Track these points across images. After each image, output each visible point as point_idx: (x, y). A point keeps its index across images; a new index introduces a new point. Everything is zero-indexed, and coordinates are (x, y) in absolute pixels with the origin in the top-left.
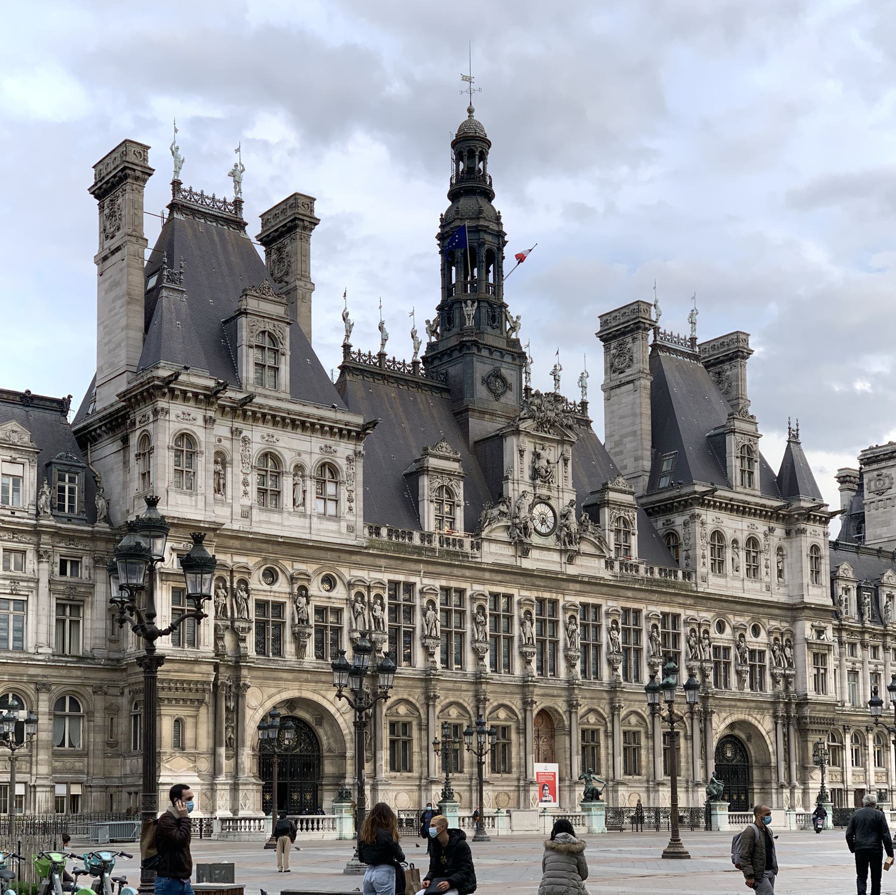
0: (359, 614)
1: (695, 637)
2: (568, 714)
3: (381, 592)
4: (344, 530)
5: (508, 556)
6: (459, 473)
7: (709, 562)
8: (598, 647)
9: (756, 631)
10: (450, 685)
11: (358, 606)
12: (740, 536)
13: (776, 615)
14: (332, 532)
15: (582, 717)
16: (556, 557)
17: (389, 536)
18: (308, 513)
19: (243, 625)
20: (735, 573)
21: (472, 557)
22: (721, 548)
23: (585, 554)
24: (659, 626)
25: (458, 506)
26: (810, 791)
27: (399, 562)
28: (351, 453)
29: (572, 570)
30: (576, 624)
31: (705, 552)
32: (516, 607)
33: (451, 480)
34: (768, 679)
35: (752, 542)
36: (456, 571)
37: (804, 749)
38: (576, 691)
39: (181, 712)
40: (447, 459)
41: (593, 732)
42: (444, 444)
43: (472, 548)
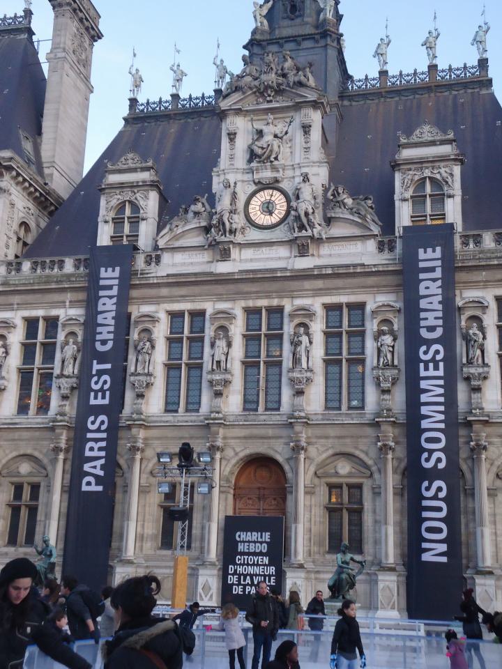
2: (292, 463)
5: (203, 263)
6: (143, 182)
8: (358, 360)
15: (322, 465)
16: (283, 252)
17: (34, 269)
21: (141, 274)
25: (143, 219)
30: (308, 334)
32: (207, 324)
33: (135, 193)
38: (298, 428)
41: (350, 486)
42: (130, 156)
43: (148, 263)
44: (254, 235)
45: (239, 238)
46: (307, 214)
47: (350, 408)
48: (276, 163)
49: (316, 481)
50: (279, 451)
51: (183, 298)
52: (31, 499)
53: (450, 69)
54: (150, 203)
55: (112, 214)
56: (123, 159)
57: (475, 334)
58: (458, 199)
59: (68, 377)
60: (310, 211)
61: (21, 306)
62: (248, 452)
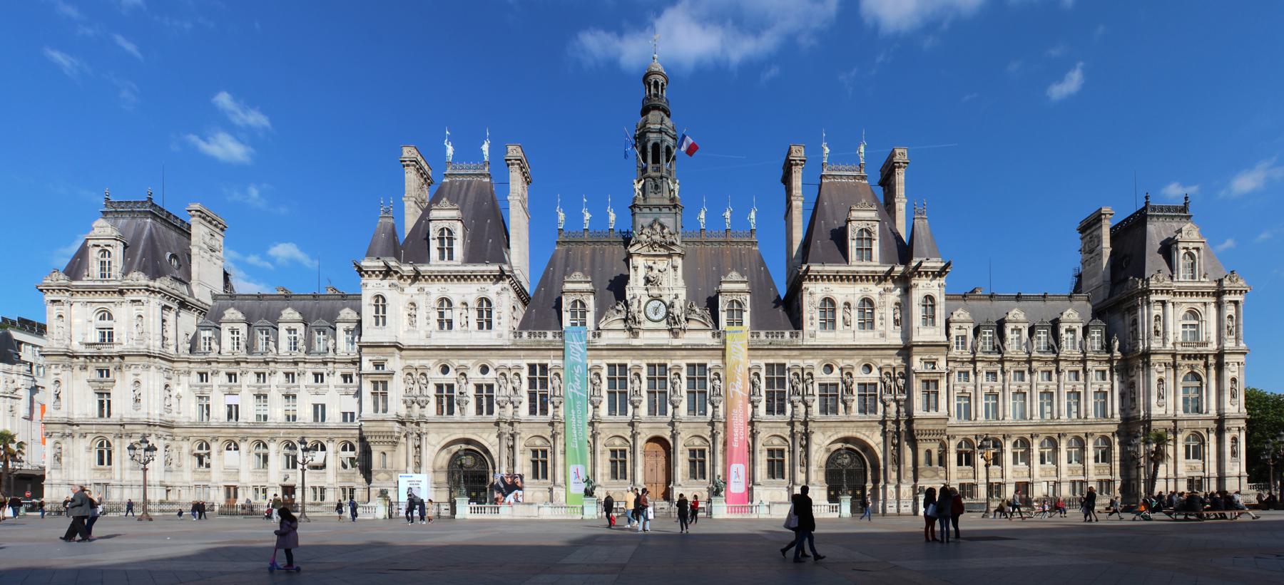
0: (500, 386)
1: (798, 378)
3: (518, 371)
7: (817, 322)
9: (868, 368)
11: (501, 381)
12: (852, 298)
13: (889, 355)
14: (486, 339)
16: (666, 335)
17: (530, 336)
18: (469, 329)
19: (422, 399)
20: (846, 327)
22: (834, 311)
24: (763, 374)
27: (535, 352)
28: (500, 289)
29: (676, 342)
30: (679, 378)
31: (814, 315)
34: (880, 405)
35: (867, 301)
38: (676, 424)
39: (384, 449)
40: (581, 282)
41: (699, 450)
42: (577, 273)
43: (594, 337)
45: (642, 326)
46: (678, 316)
47: (699, 414)
48: (660, 286)
49: (684, 448)
50: (667, 434)
51: (615, 356)
52: (542, 457)
54: (590, 302)
55: (570, 307)
56: (573, 275)
58: (748, 312)
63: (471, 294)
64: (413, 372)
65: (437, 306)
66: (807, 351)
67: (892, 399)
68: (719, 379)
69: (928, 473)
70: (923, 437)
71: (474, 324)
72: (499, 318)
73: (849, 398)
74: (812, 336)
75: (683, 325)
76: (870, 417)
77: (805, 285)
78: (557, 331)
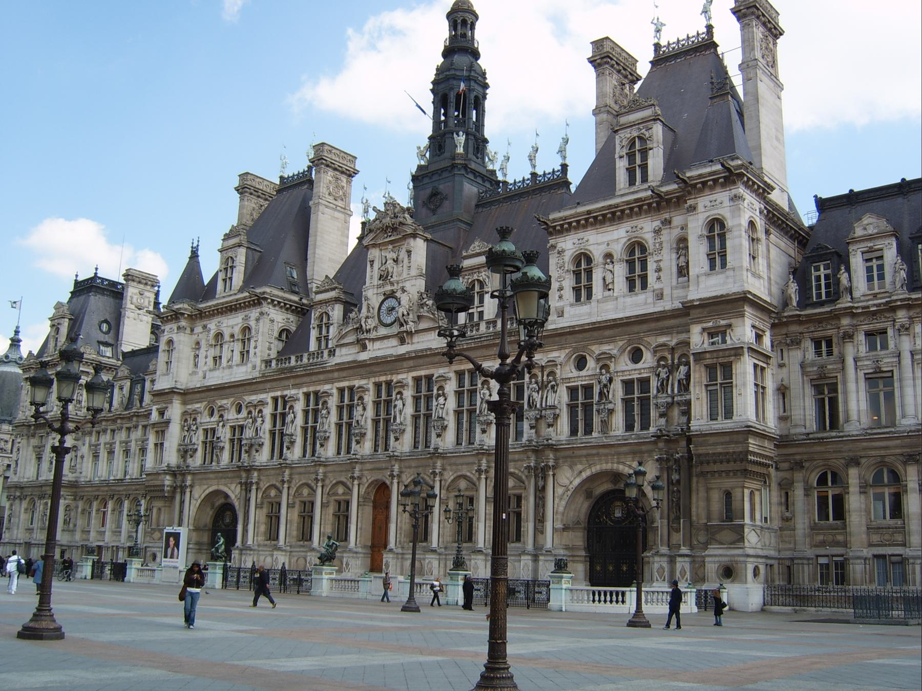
1: (536, 383)
4: (250, 370)
9: (636, 356)
10: (302, 470)
13: (667, 328)
14: (243, 373)
16: (394, 342)
17: (277, 364)
20: (607, 293)
23: (417, 332)
26: (707, 559)
28: (258, 314)
29: (403, 350)
30: (401, 398)
36: (314, 378)
37: (708, 500)
43: (329, 355)
44: (383, 331)
46: (403, 315)
53: (545, 174)
54: (337, 312)
57: (484, 394)
59: (288, 435)
60: (405, 313)
61: (272, 389)
62: (373, 479)
63: (237, 325)
64: (188, 417)
65: (214, 343)
66: (551, 340)
67: (668, 403)
68: (444, 395)
69: (726, 535)
70: (716, 468)
71: (237, 357)
72: (255, 348)
73: (602, 407)
74: (561, 314)
75: (411, 326)
76: (638, 437)
77: (552, 242)
78: (299, 355)
